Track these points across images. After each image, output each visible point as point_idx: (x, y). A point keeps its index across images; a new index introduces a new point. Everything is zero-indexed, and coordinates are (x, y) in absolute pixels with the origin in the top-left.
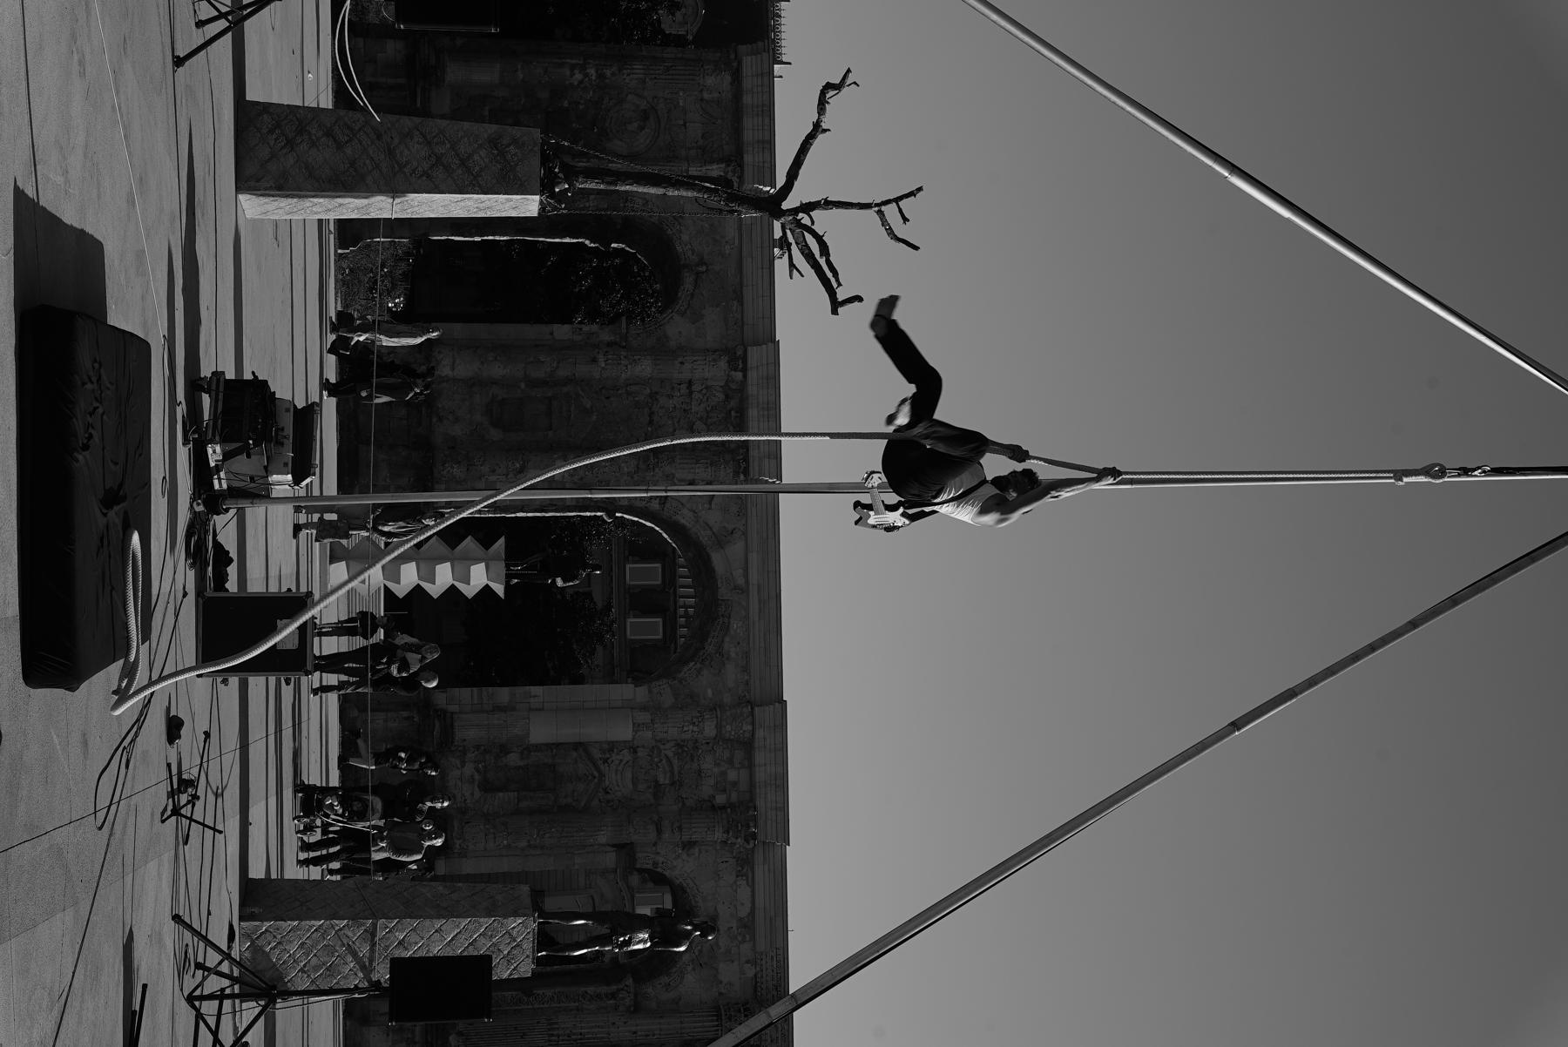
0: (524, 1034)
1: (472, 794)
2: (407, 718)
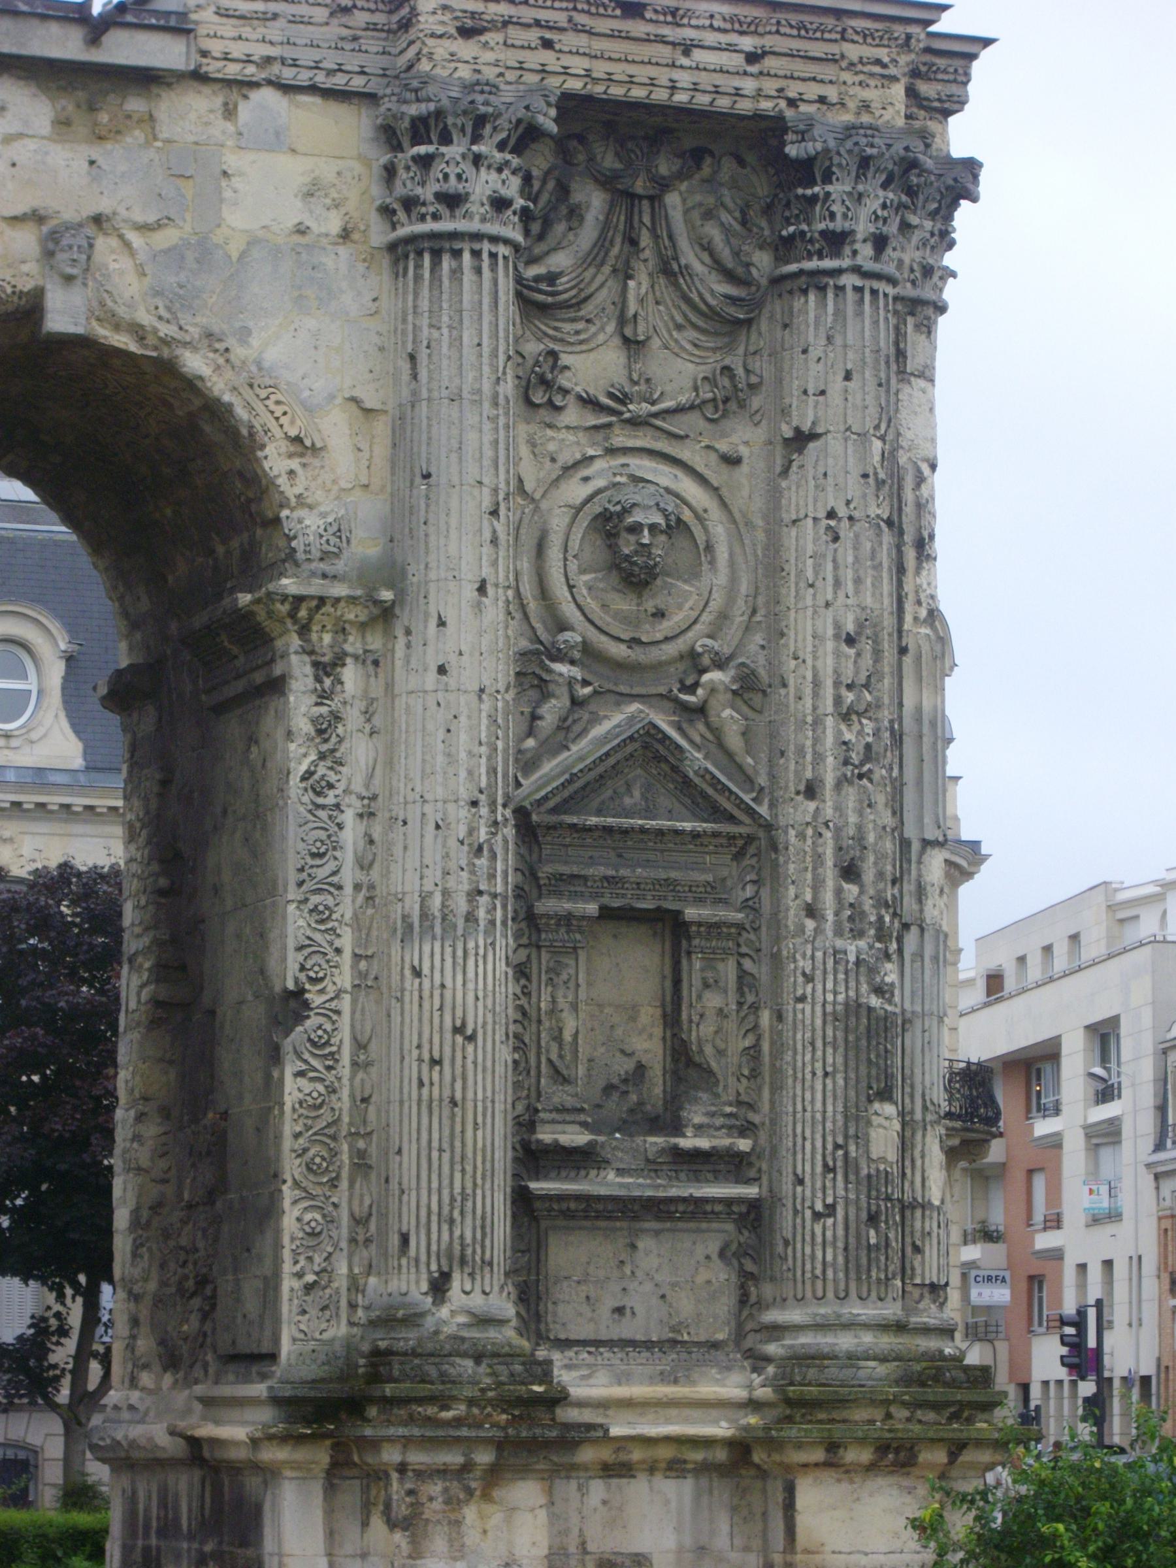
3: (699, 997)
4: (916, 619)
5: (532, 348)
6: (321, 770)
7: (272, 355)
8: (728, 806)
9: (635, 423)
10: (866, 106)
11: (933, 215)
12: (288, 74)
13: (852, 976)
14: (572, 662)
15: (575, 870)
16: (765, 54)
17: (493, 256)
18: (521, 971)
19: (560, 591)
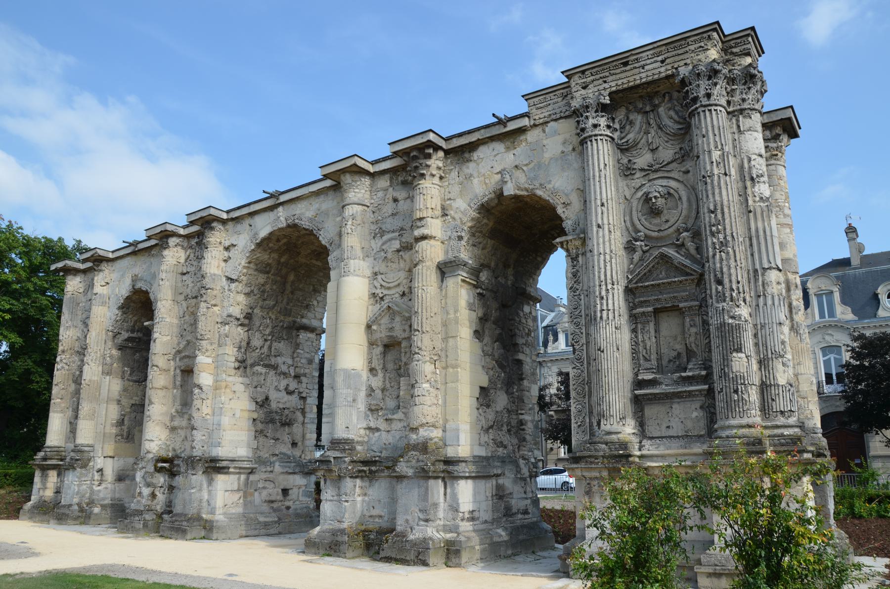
0: (599, 350)
1: (400, 420)
2: (325, 481)
3: (689, 330)
4: (754, 201)
5: (625, 161)
6: (575, 286)
7: (557, 185)
8: (689, 271)
9: (656, 171)
10: (700, 60)
11: (745, 84)
12: (554, 117)
13: (721, 314)
14: (642, 241)
15: (645, 299)
16: (666, 59)
17: (596, 140)
18: (634, 331)
19: (637, 222)
